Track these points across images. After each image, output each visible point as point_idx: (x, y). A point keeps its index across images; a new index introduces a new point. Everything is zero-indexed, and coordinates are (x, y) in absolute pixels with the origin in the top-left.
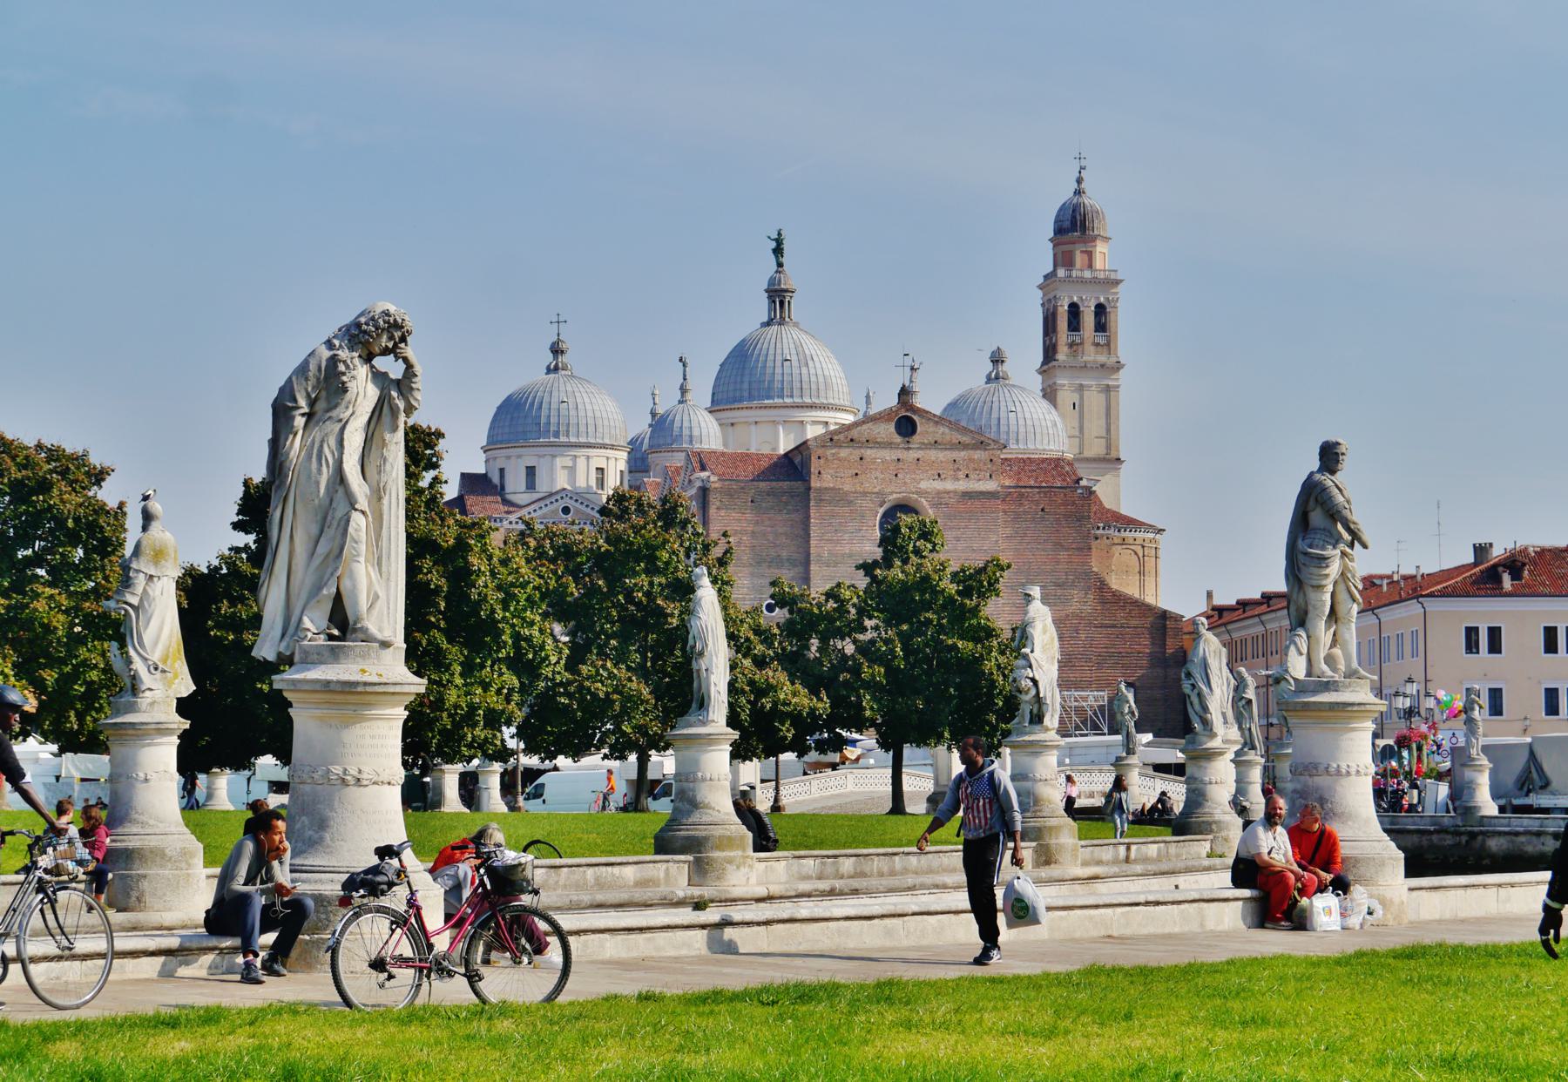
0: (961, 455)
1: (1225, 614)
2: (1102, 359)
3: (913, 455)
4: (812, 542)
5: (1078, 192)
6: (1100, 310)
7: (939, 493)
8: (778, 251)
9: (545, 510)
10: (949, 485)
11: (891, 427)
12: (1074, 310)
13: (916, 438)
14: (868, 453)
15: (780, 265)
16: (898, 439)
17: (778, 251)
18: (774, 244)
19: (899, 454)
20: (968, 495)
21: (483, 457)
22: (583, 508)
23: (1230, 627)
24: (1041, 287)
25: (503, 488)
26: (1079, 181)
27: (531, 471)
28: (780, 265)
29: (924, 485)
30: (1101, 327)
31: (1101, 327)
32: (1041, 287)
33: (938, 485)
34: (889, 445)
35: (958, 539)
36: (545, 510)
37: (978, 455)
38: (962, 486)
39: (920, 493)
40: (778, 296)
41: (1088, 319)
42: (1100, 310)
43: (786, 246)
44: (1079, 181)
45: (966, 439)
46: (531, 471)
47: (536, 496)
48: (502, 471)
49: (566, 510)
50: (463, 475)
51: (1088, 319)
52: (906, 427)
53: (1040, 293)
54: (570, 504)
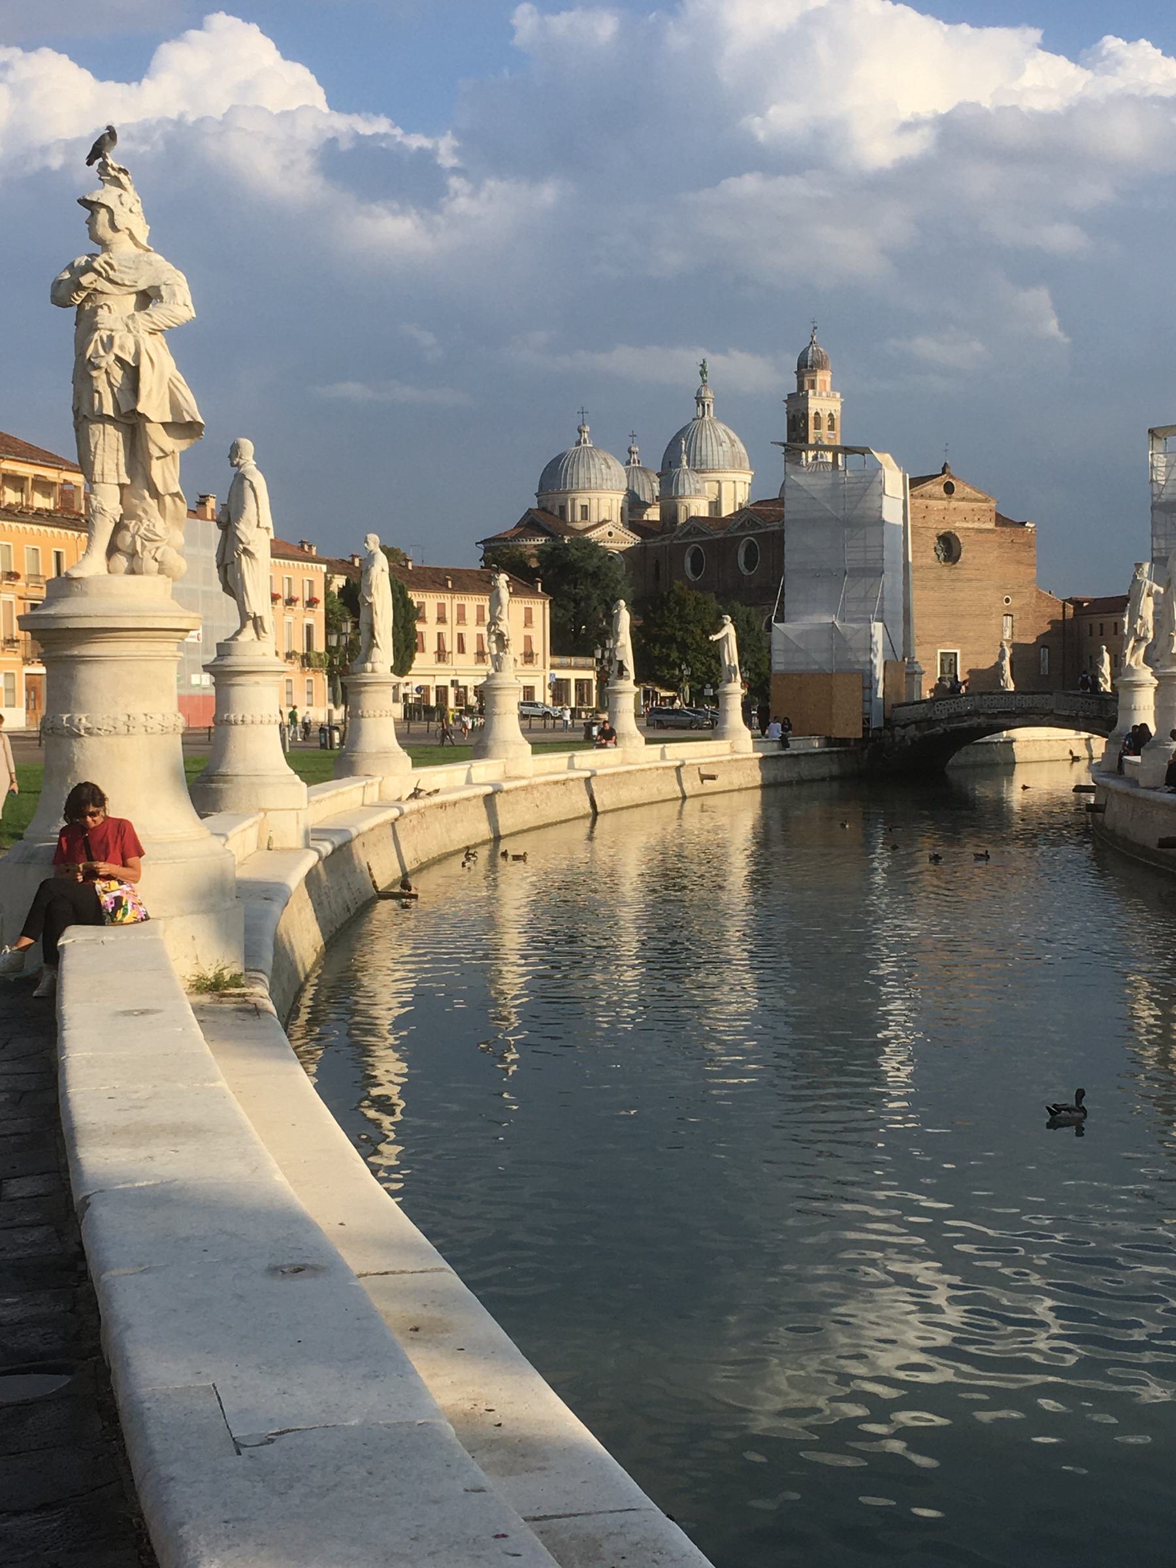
0: (975, 505)
3: (954, 504)
10: (970, 525)
14: (931, 503)
16: (945, 495)
19: (945, 503)
20: (979, 531)
27: (585, 508)
28: (704, 381)
29: (957, 525)
30: (831, 428)
31: (831, 428)
33: (966, 525)
34: (941, 499)
35: (974, 558)
37: (984, 506)
38: (976, 525)
41: (825, 423)
49: (610, 534)
51: (825, 423)
52: (949, 489)
54: (613, 530)
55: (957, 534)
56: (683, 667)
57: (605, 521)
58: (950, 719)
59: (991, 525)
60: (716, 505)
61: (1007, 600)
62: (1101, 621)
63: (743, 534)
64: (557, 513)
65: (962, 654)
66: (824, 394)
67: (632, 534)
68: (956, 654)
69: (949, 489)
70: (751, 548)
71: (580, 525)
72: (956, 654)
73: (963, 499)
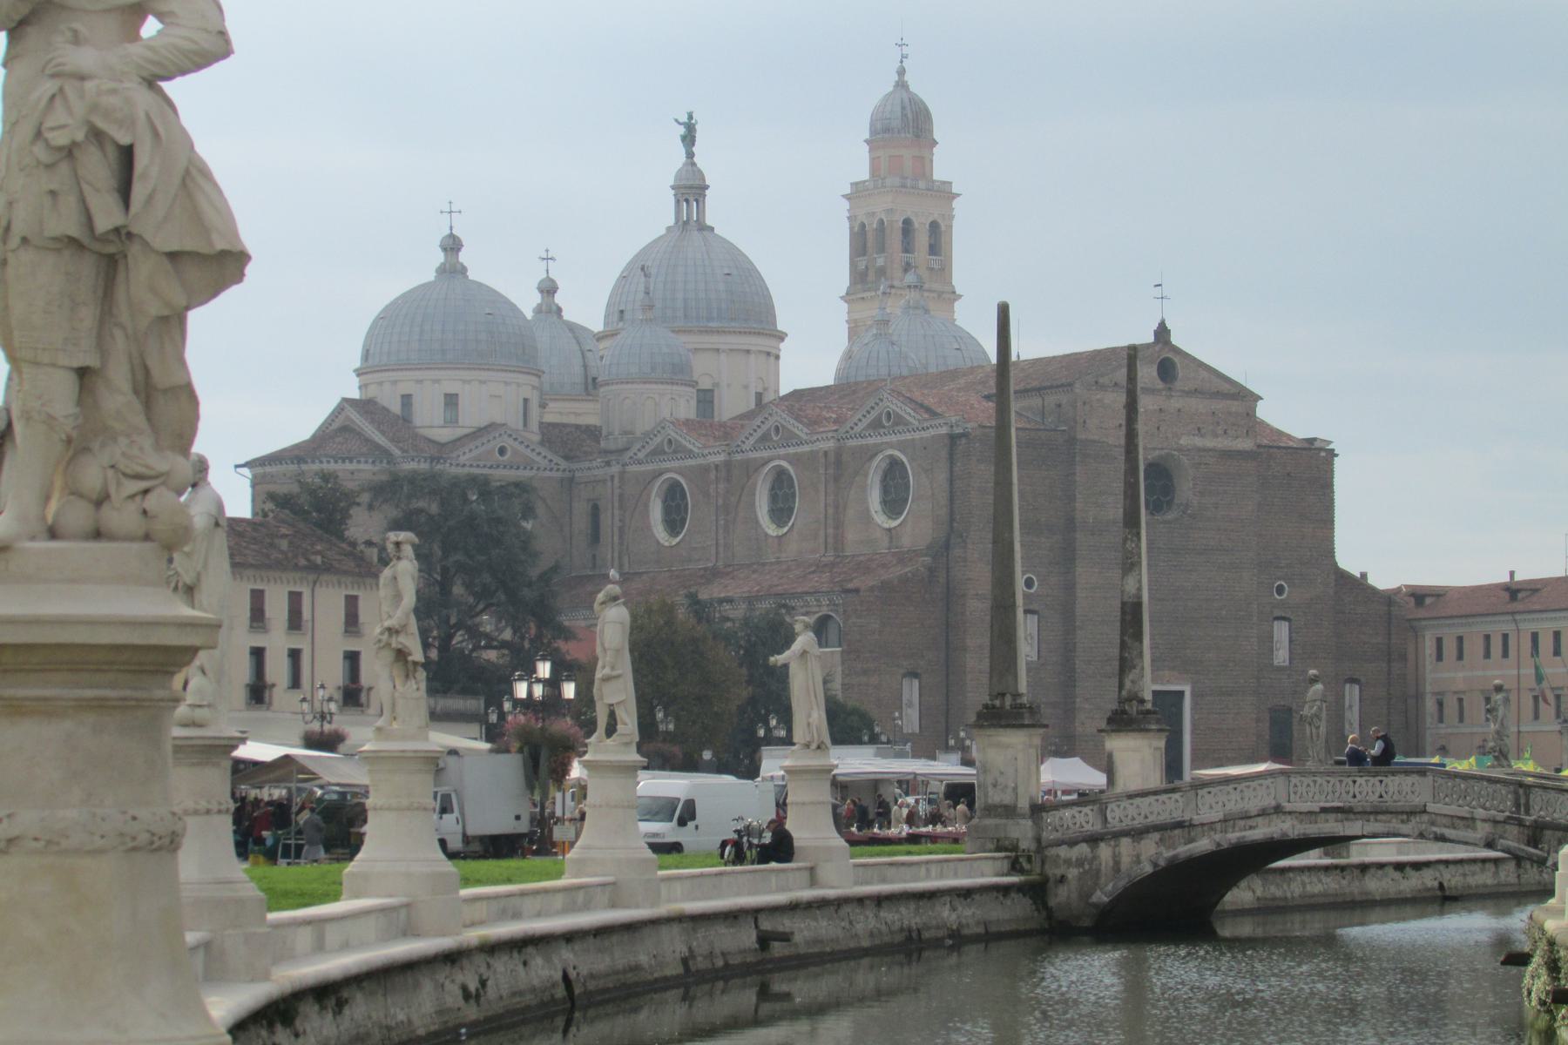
0: (1219, 405)
1: (1428, 601)
2: (935, 286)
3: (1176, 403)
4: (1078, 505)
5: (901, 85)
6: (934, 226)
7: (1199, 450)
8: (689, 138)
9: (481, 449)
10: (1209, 443)
11: (1155, 374)
12: (907, 227)
13: (1178, 385)
15: (690, 155)
16: (1160, 385)
17: (689, 138)
18: (682, 130)
20: (1227, 455)
21: (356, 381)
22: (521, 448)
23: (1518, 617)
24: (847, 197)
25: (406, 419)
26: (902, 72)
27: (451, 401)
28: (690, 155)
31: (934, 249)
32: (847, 197)
33: (1199, 442)
36: (481, 449)
37: (1235, 406)
39: (1180, 450)
40: (691, 190)
41: (922, 239)
42: (934, 226)
43: (698, 136)
44: (902, 72)
45: (1225, 387)
46: (451, 401)
47: (459, 432)
48: (407, 400)
49: (502, 451)
50: (345, 400)
51: (922, 239)
53: (846, 205)
54: (508, 443)
55: (1184, 459)
56: (773, 722)
57: (491, 427)
58: (1228, 821)
59: (1245, 444)
60: (706, 399)
61: (1280, 590)
62: (1460, 631)
63: (766, 454)
64: (396, 408)
65: (1193, 694)
66: (922, 184)
67: (544, 452)
68: (1182, 693)
69: (1167, 370)
70: (781, 481)
71: (444, 435)
72: (1182, 693)
73: (1196, 392)
